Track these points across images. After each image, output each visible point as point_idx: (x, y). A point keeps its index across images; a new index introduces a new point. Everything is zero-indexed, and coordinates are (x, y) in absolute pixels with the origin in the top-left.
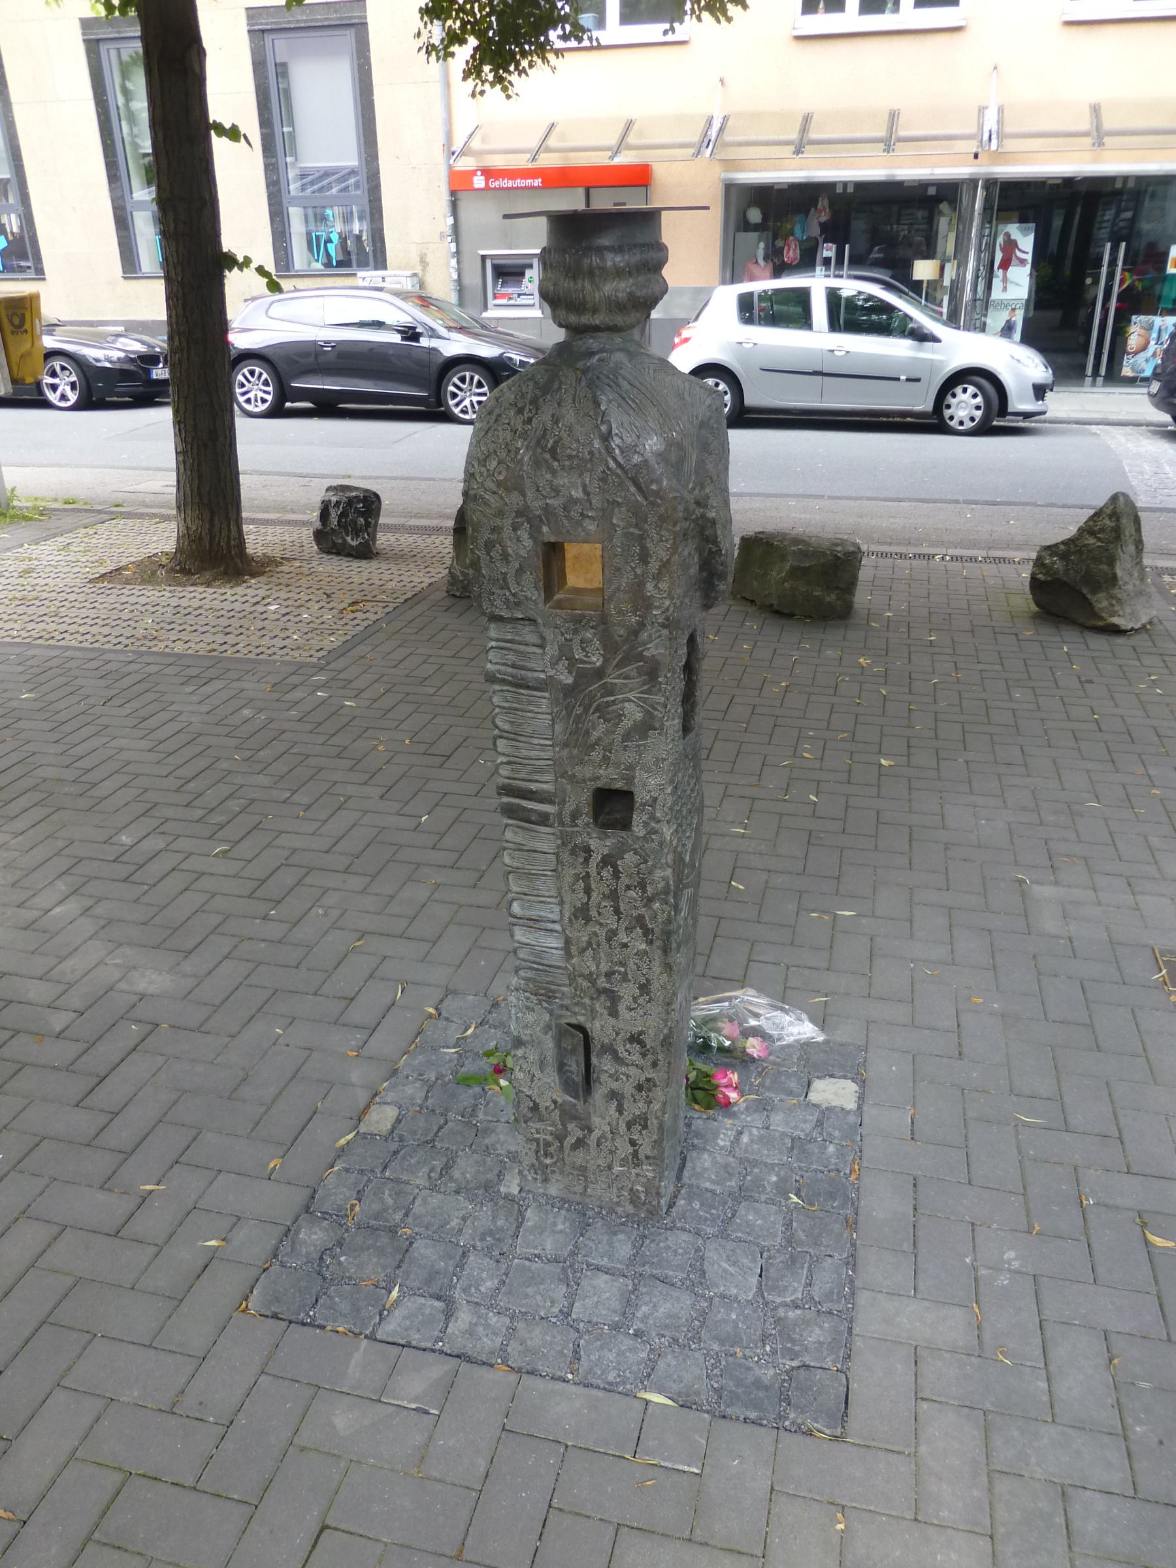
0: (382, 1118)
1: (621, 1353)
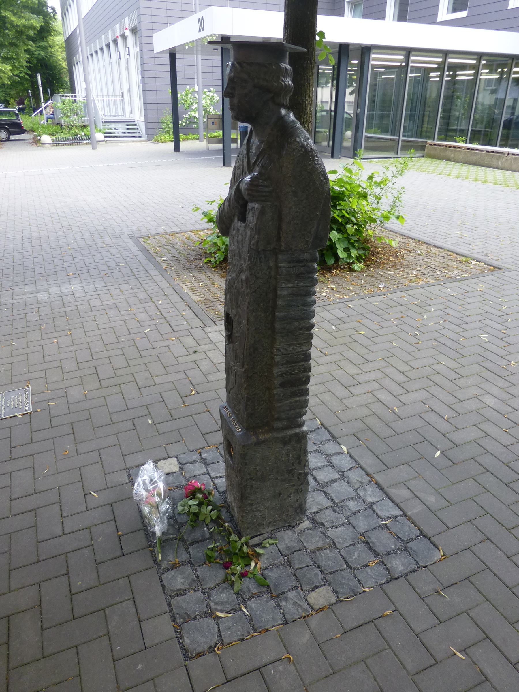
0: (321, 597)
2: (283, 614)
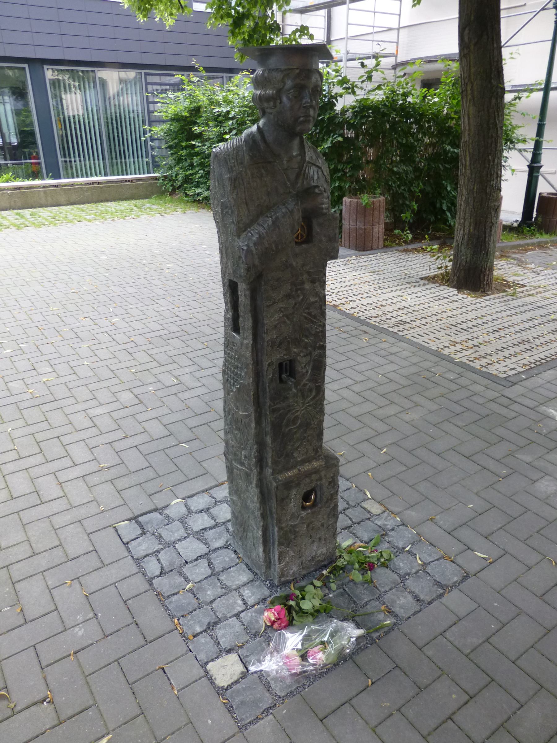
1: (199, 503)
2: (398, 526)
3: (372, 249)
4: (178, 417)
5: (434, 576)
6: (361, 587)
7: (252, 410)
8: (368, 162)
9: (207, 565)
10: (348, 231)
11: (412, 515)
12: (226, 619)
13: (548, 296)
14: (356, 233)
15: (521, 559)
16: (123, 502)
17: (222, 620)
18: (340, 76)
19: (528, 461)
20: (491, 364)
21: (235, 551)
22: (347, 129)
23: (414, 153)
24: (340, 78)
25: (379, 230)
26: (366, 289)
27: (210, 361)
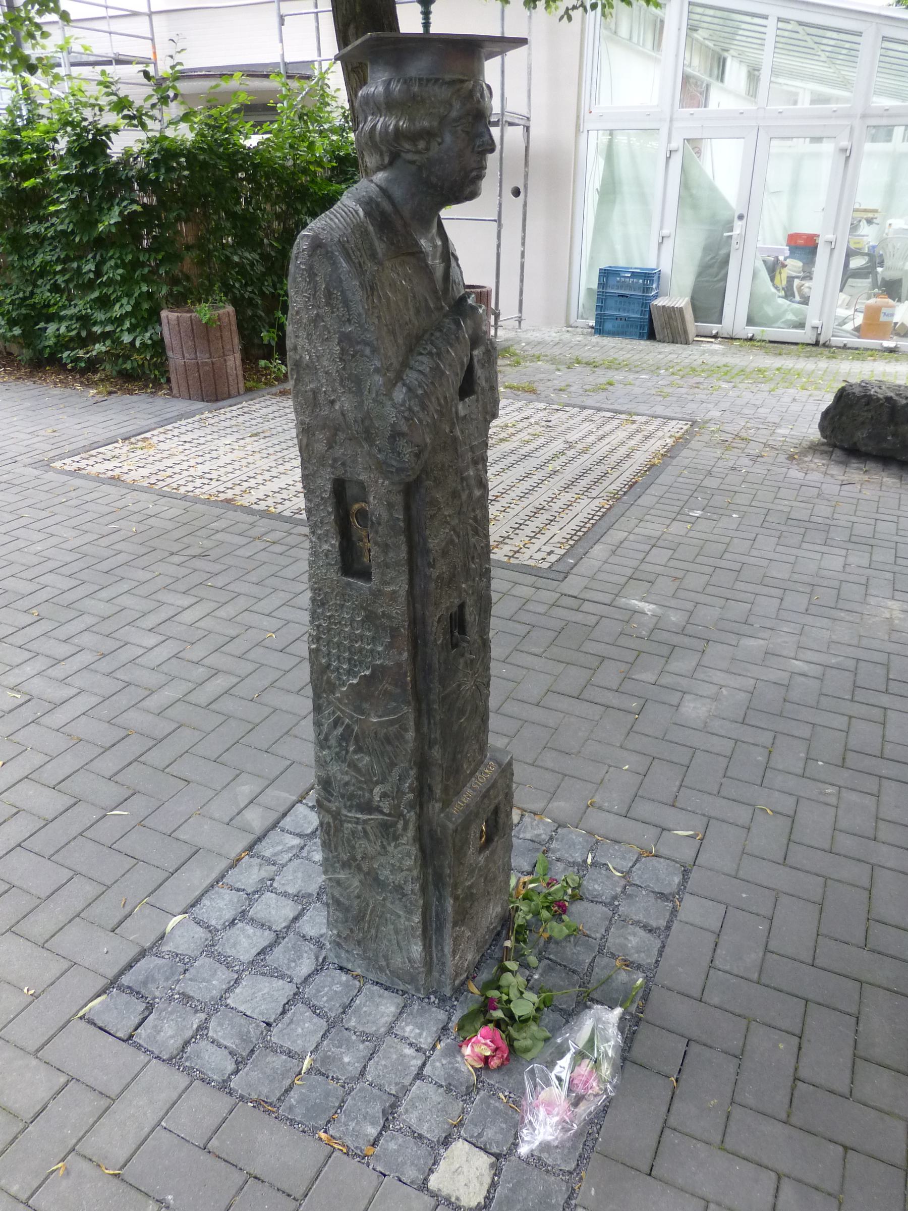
1: (220, 910)
3: (230, 396)
4: (68, 764)
5: (649, 886)
6: (568, 944)
7: (408, 711)
8: (188, 248)
9: (309, 1013)
10: (181, 370)
11: (562, 807)
12: (406, 1090)
13: (526, 438)
14: (198, 371)
15: (731, 821)
16: (65, 964)
17: (401, 1095)
18: (116, 95)
19: (653, 681)
20: (518, 552)
21: (341, 968)
22: (140, 191)
23: (257, 230)
24: (115, 98)
25: (234, 361)
26: (264, 464)
27: (65, 641)
